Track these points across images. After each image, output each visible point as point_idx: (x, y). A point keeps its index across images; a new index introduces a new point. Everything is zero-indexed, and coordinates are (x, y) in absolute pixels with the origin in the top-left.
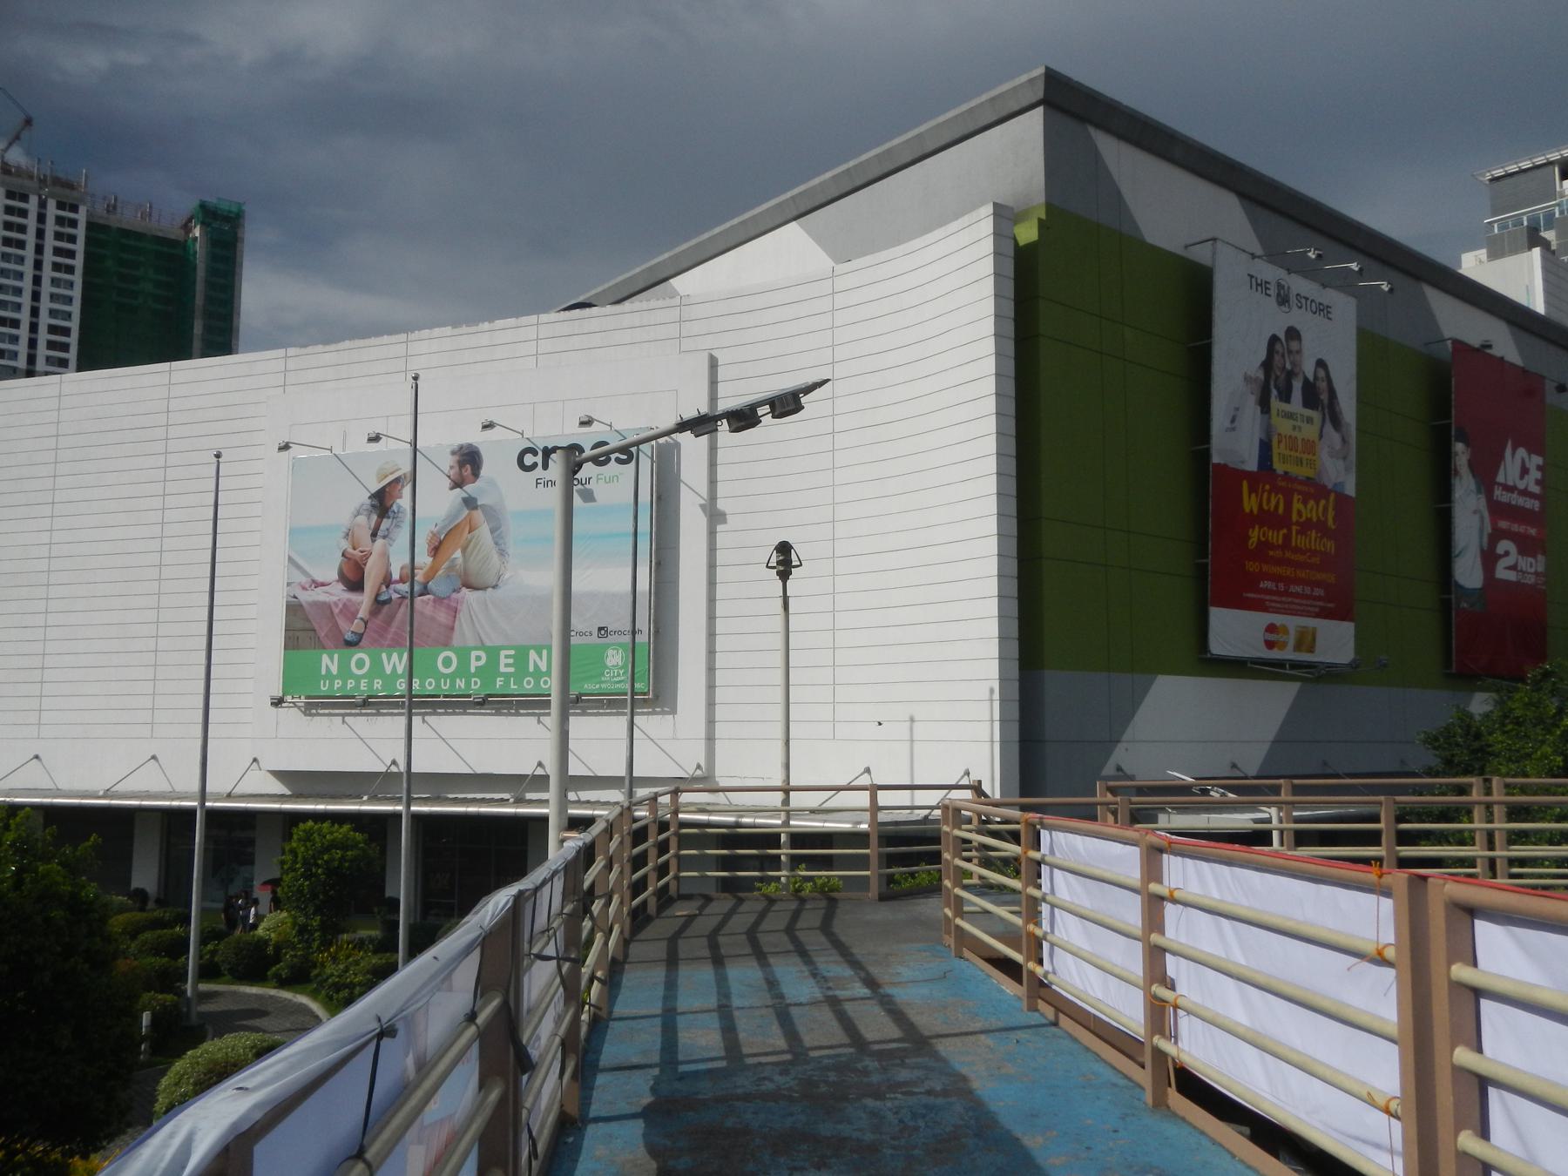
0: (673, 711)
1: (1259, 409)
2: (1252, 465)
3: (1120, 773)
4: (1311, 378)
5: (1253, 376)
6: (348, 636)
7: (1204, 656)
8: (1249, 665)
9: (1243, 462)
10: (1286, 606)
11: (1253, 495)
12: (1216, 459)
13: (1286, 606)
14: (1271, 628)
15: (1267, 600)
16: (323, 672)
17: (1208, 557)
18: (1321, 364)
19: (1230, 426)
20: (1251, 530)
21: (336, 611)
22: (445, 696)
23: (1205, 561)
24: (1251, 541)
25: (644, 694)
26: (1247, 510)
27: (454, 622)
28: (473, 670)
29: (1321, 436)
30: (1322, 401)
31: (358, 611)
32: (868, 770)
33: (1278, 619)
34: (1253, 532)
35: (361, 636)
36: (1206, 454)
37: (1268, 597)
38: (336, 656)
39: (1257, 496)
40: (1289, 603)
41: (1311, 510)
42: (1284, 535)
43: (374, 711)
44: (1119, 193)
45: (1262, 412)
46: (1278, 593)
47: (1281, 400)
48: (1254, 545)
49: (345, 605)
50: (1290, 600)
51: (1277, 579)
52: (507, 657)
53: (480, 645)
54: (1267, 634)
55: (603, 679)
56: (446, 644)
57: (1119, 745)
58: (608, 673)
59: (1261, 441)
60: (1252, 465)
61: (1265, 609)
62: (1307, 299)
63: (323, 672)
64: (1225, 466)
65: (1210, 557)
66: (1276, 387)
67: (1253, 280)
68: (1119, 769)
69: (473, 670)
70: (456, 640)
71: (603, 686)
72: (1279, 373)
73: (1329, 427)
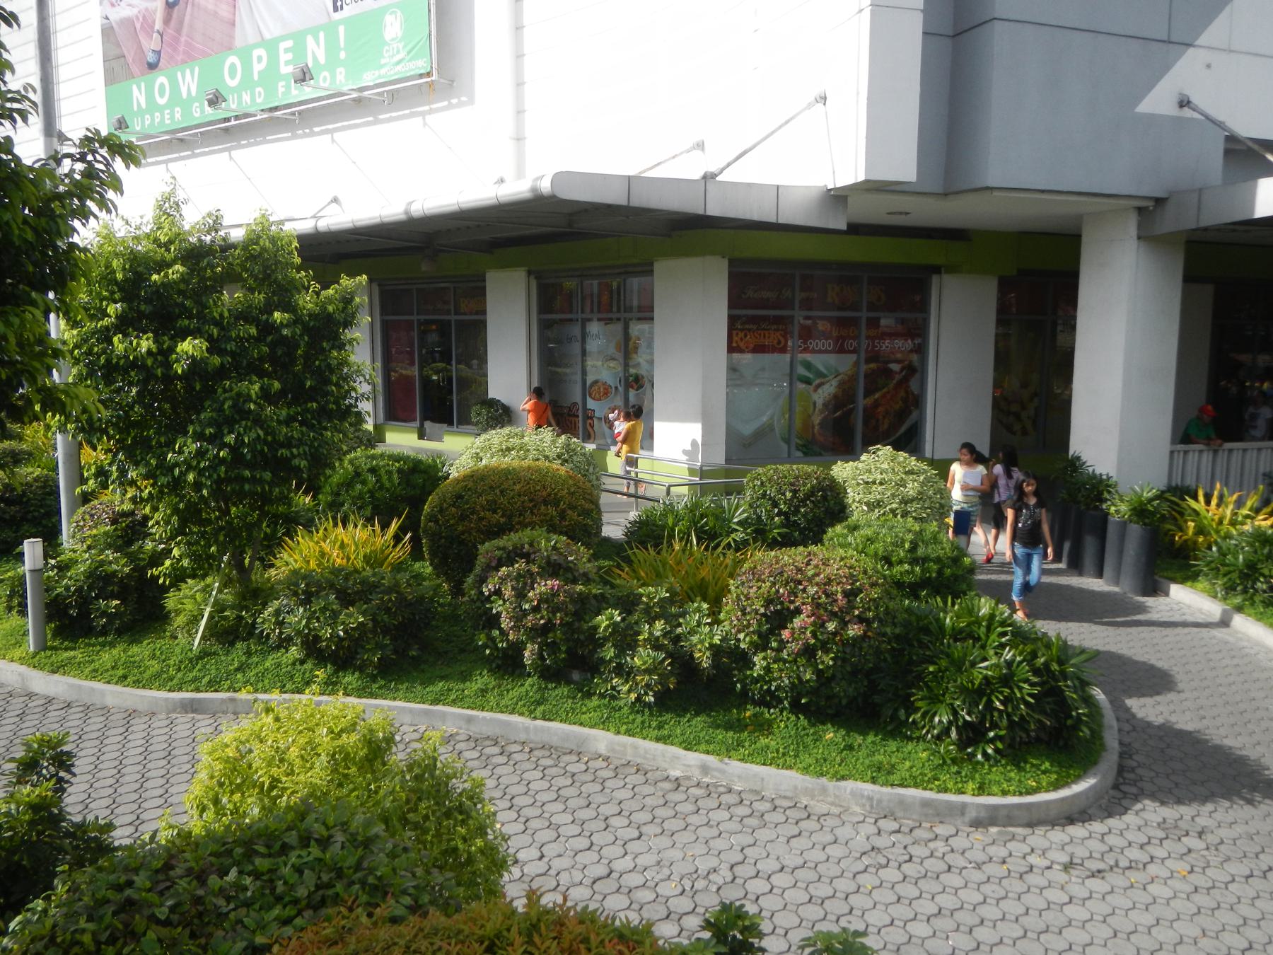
0: (471, 101)
3: (1187, 113)
6: (151, 58)
16: (135, 108)
21: (138, 26)
22: (237, 118)
25: (429, 74)
27: (234, 14)
28: (256, 77)
31: (154, 22)
32: (700, 146)
35: (159, 53)
38: (143, 85)
43: (189, 153)
49: (144, 17)
52: (286, 50)
53: (260, 39)
55: (383, 61)
56: (229, 48)
57: (1191, 51)
58: (387, 51)
63: (135, 108)
68: (1184, 103)
69: (256, 77)
70: (238, 42)
71: (383, 71)
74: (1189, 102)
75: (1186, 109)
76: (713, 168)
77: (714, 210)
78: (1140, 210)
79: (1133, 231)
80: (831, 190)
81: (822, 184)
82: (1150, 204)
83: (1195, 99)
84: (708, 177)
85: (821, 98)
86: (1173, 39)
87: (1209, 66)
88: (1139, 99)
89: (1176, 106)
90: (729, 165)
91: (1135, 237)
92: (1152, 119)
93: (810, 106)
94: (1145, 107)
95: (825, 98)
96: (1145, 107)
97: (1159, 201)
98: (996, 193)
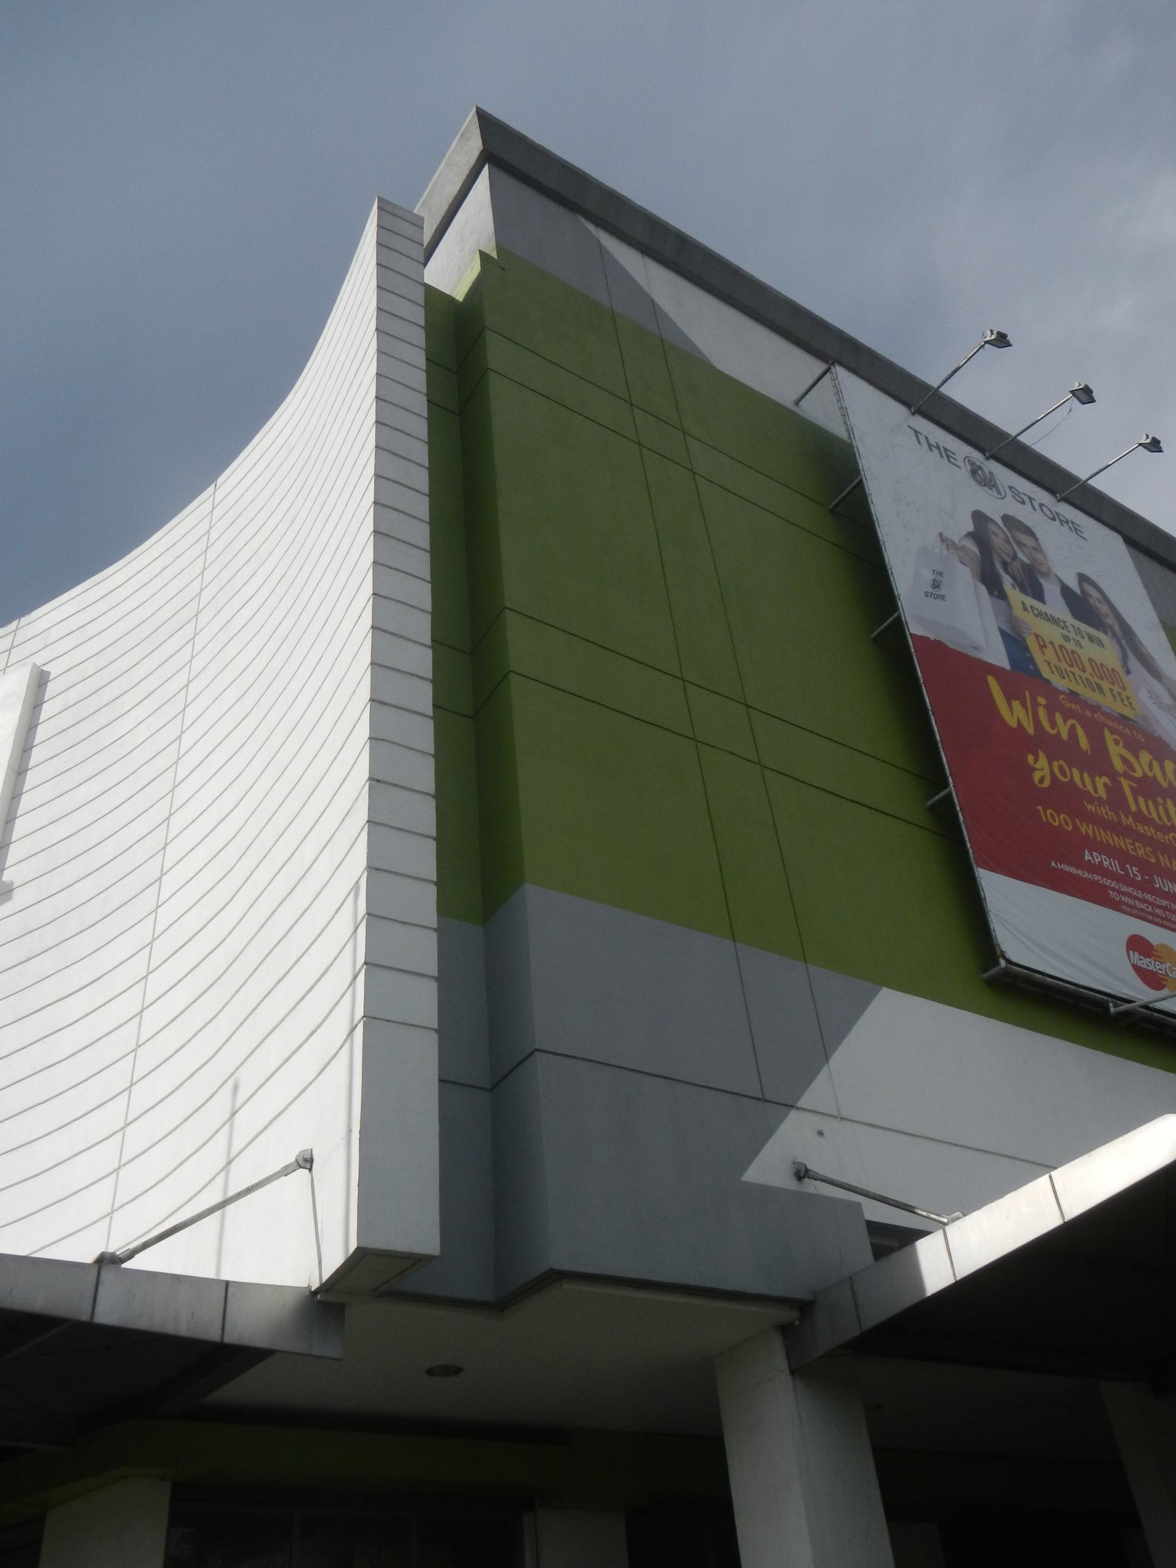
1: (983, 589)
2: (997, 655)
3: (811, 1186)
4: (1076, 589)
5: (957, 542)
7: (993, 971)
8: (1112, 1010)
9: (976, 648)
10: (1159, 911)
11: (1016, 704)
12: (914, 628)
13: (1159, 911)
14: (1137, 944)
15: (1113, 889)
17: (946, 785)
18: (1082, 578)
19: (931, 590)
20: (1030, 758)
23: (946, 791)
24: (1037, 776)
26: (1013, 724)
29: (1128, 672)
30: (1110, 627)
33: (1154, 934)
34: (1036, 760)
36: (899, 627)
37: (1108, 882)
39: (1024, 705)
40: (1161, 907)
41: (1151, 766)
42: (1105, 785)
44: (653, 302)
45: (991, 593)
46: (1127, 880)
47: (1023, 590)
48: (1046, 784)
50: (1164, 903)
51: (1124, 857)
54: (1136, 957)
57: (793, 1114)
59: (1003, 633)
60: (997, 655)
61: (1115, 906)
62: (1030, 499)
64: (938, 643)
65: (950, 780)
66: (1007, 572)
67: (922, 438)
68: (802, 1174)
72: (1008, 560)
73: (1133, 663)
74: (807, 1171)
75: (806, 1180)
76: (116, 1246)
77: (108, 1314)
78: (785, 1330)
79: (780, 1361)
80: (315, 1293)
81: (303, 1284)
82: (790, 1315)
83: (814, 1167)
84: (107, 1261)
85: (305, 1160)
86: (767, 1097)
87: (821, 1133)
88: (744, 1166)
89: (795, 1179)
90: (146, 1246)
91: (787, 1372)
92: (765, 1192)
93: (286, 1171)
94: (753, 1174)
95: (311, 1161)
96: (753, 1174)
97: (805, 1307)
98: (568, 1286)
